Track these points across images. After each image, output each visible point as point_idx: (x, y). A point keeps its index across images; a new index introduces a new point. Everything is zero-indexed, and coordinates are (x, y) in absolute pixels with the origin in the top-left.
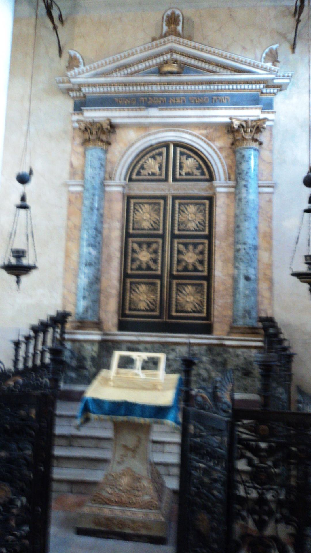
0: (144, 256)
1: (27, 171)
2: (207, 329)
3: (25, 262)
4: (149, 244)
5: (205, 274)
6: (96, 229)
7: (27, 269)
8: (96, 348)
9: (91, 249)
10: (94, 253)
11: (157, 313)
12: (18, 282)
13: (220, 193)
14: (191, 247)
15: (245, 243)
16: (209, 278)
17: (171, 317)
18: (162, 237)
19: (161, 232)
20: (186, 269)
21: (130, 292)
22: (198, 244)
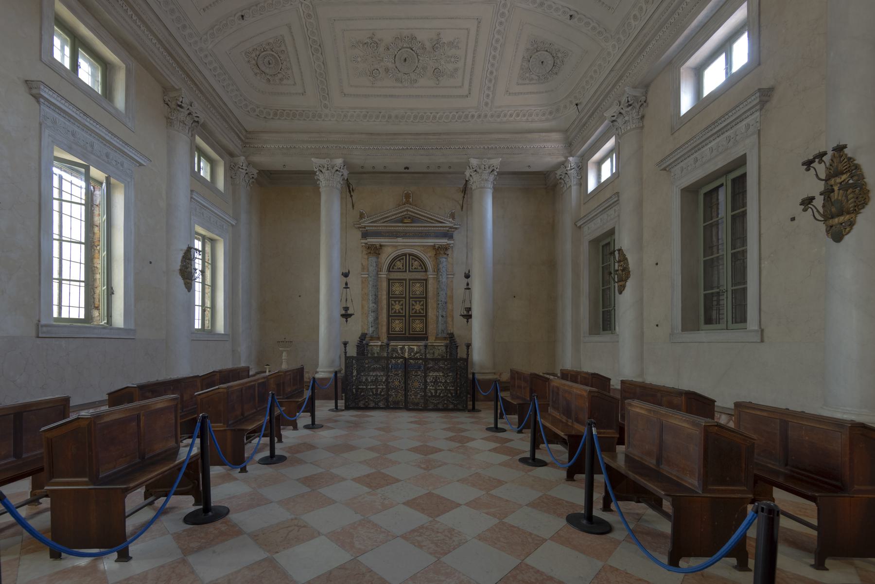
0: (397, 307)
1: (347, 271)
2: (426, 339)
3: (349, 312)
6: (375, 295)
7: (350, 315)
8: (379, 348)
10: (375, 306)
12: (347, 321)
16: (426, 316)
18: (405, 298)
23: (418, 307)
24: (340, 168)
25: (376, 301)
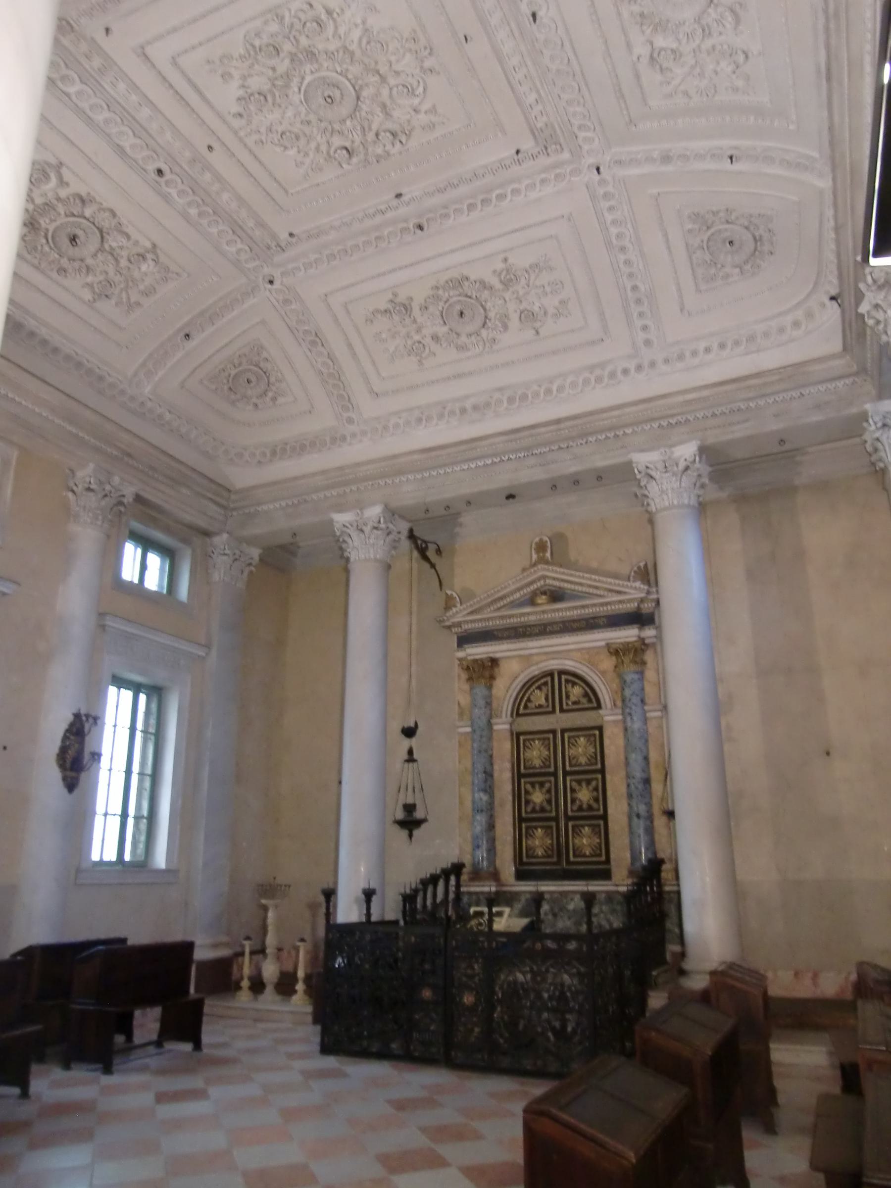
0: (538, 797)
2: (606, 875)
3: (419, 814)
4: (542, 785)
5: (601, 812)
6: (485, 772)
7: (418, 823)
9: (482, 795)
10: (485, 798)
11: (555, 859)
12: (411, 836)
13: (608, 722)
14: (584, 784)
15: (633, 778)
16: (605, 817)
17: (568, 862)
18: (555, 774)
19: (552, 769)
20: (580, 809)
21: (526, 837)
22: (592, 779)
23: (584, 795)
24: (379, 522)
25: (488, 786)
